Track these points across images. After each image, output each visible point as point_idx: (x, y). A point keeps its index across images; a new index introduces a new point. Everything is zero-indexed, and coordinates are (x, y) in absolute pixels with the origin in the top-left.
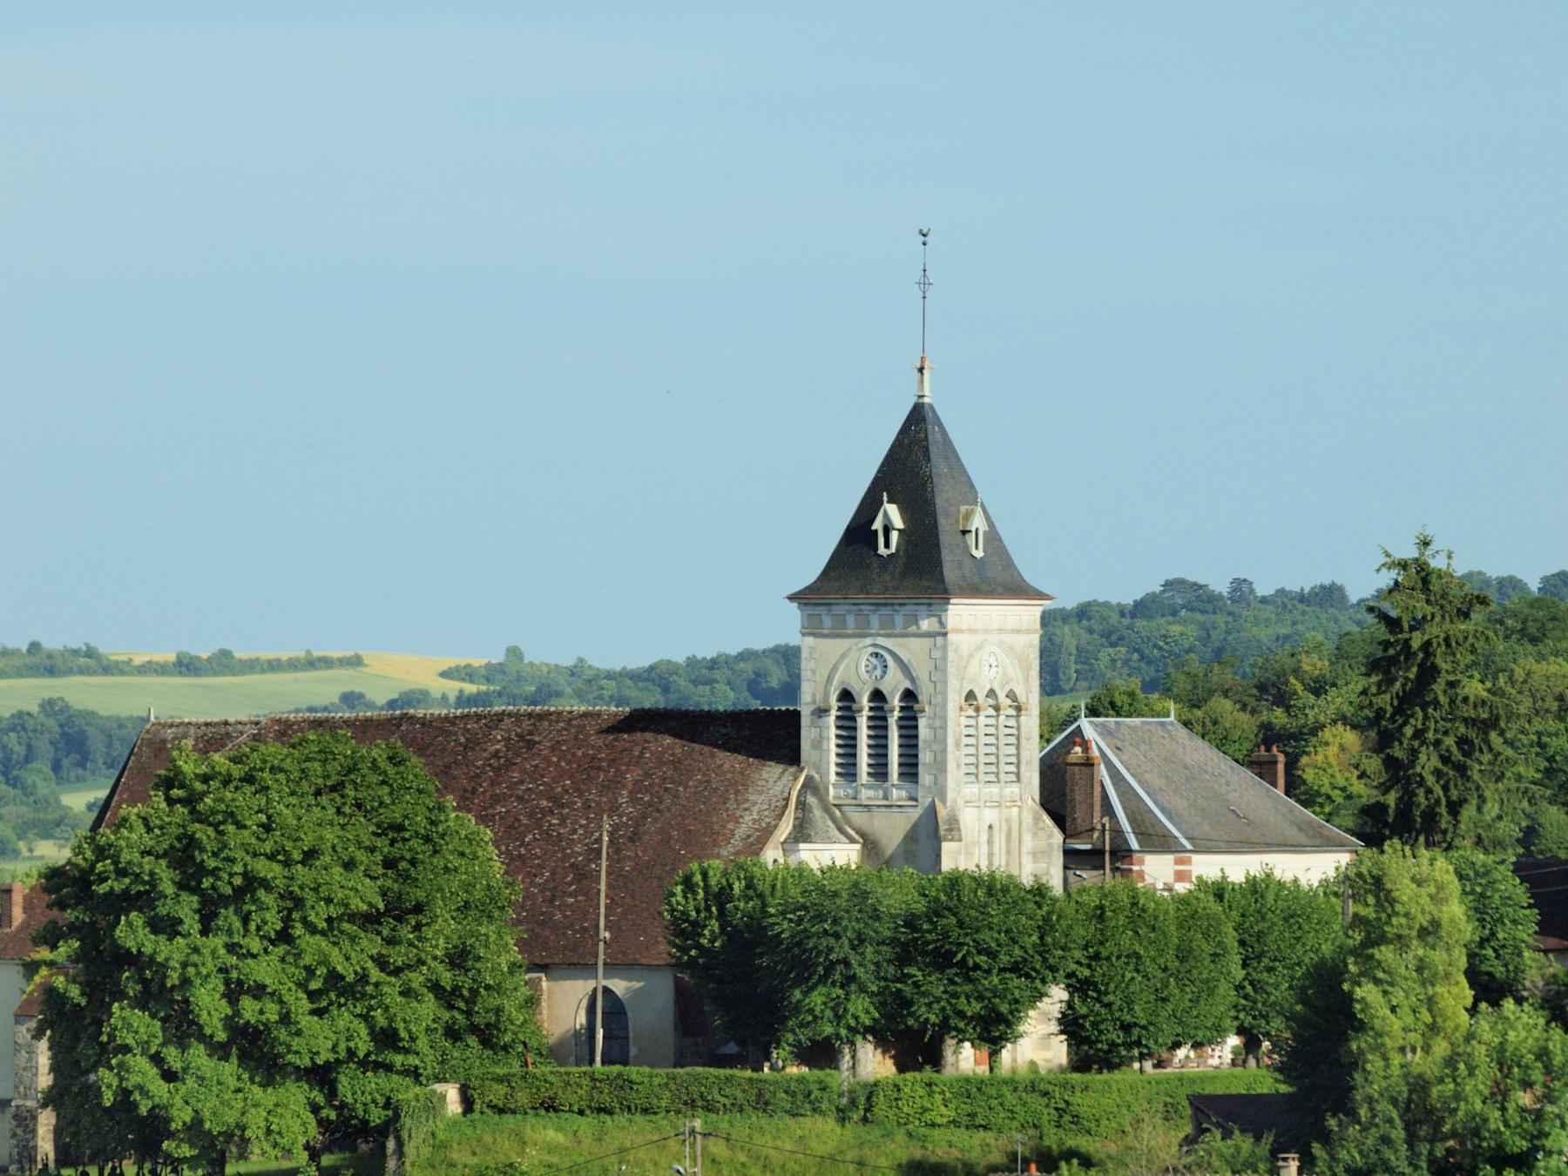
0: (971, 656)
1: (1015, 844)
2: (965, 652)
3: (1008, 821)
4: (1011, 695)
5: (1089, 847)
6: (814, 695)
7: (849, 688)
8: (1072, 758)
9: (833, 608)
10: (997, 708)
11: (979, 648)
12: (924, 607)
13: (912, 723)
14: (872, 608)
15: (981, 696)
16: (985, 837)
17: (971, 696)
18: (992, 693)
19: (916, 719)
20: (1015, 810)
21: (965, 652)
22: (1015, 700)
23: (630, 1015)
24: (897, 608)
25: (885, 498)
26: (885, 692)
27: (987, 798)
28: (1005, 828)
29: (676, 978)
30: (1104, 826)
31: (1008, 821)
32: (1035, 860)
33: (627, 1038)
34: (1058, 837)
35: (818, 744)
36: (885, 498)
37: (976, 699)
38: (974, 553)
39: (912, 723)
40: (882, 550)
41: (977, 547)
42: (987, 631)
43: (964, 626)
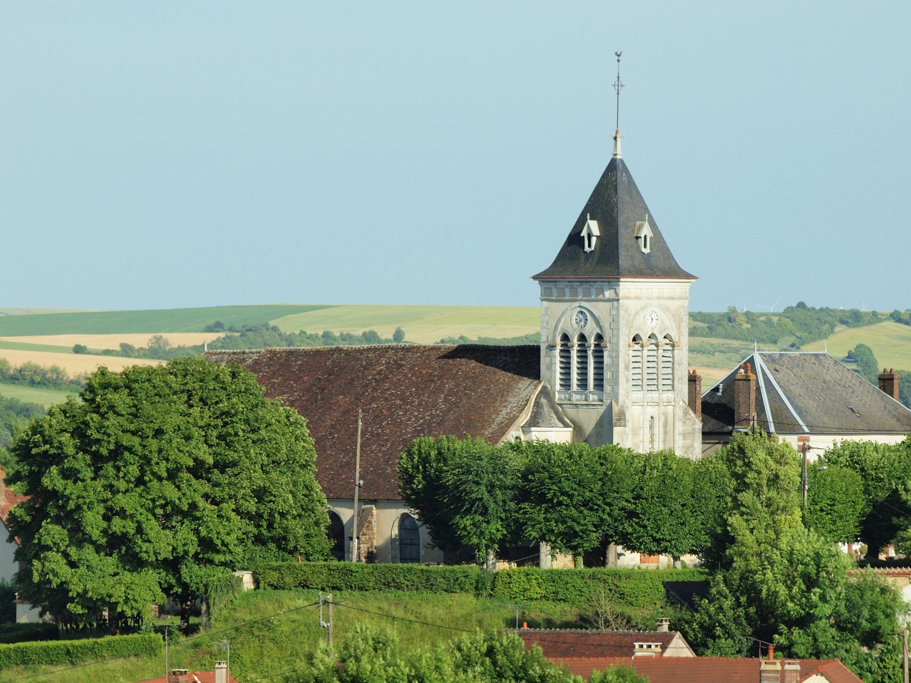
1: (670, 428)
14: (578, 284)
20: (670, 408)
24: (592, 284)
25: (588, 217)
26: (586, 335)
28: (663, 419)
31: (665, 415)
33: (419, 544)
36: (588, 217)
38: (644, 250)
39: (601, 354)
40: (587, 249)
41: (645, 246)
42: (649, 298)
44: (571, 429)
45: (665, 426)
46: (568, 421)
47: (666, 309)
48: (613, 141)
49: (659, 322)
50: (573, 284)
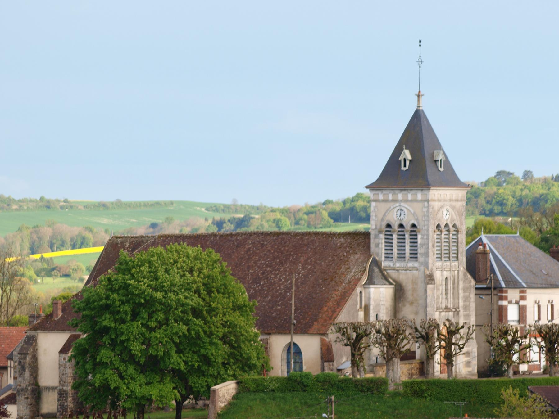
0: (439, 210)
1: (456, 285)
2: (436, 208)
3: (454, 277)
4: (454, 226)
5: (485, 286)
6: (376, 225)
7: (390, 223)
8: (478, 251)
9: (384, 191)
10: (449, 231)
11: (442, 207)
12: (420, 191)
13: (415, 237)
14: (399, 191)
15: (443, 226)
16: (444, 283)
17: (438, 226)
18: (447, 225)
19: (416, 235)
20: (456, 272)
21: (436, 208)
22: (456, 228)
23: (303, 353)
24: (409, 191)
25: (404, 147)
26: (404, 225)
27: (445, 267)
28: (452, 279)
29: (321, 338)
30: (491, 278)
31: (454, 277)
32: (464, 292)
34: (473, 282)
35: (377, 245)
36: (404, 147)
37: (441, 227)
38: (440, 169)
39: (415, 237)
41: (441, 167)
42: (445, 200)
43: (436, 198)
44: (393, 286)
45: (454, 284)
46: (391, 281)
47: (453, 208)
48: (416, 97)
49: (450, 216)
50: (395, 191)
